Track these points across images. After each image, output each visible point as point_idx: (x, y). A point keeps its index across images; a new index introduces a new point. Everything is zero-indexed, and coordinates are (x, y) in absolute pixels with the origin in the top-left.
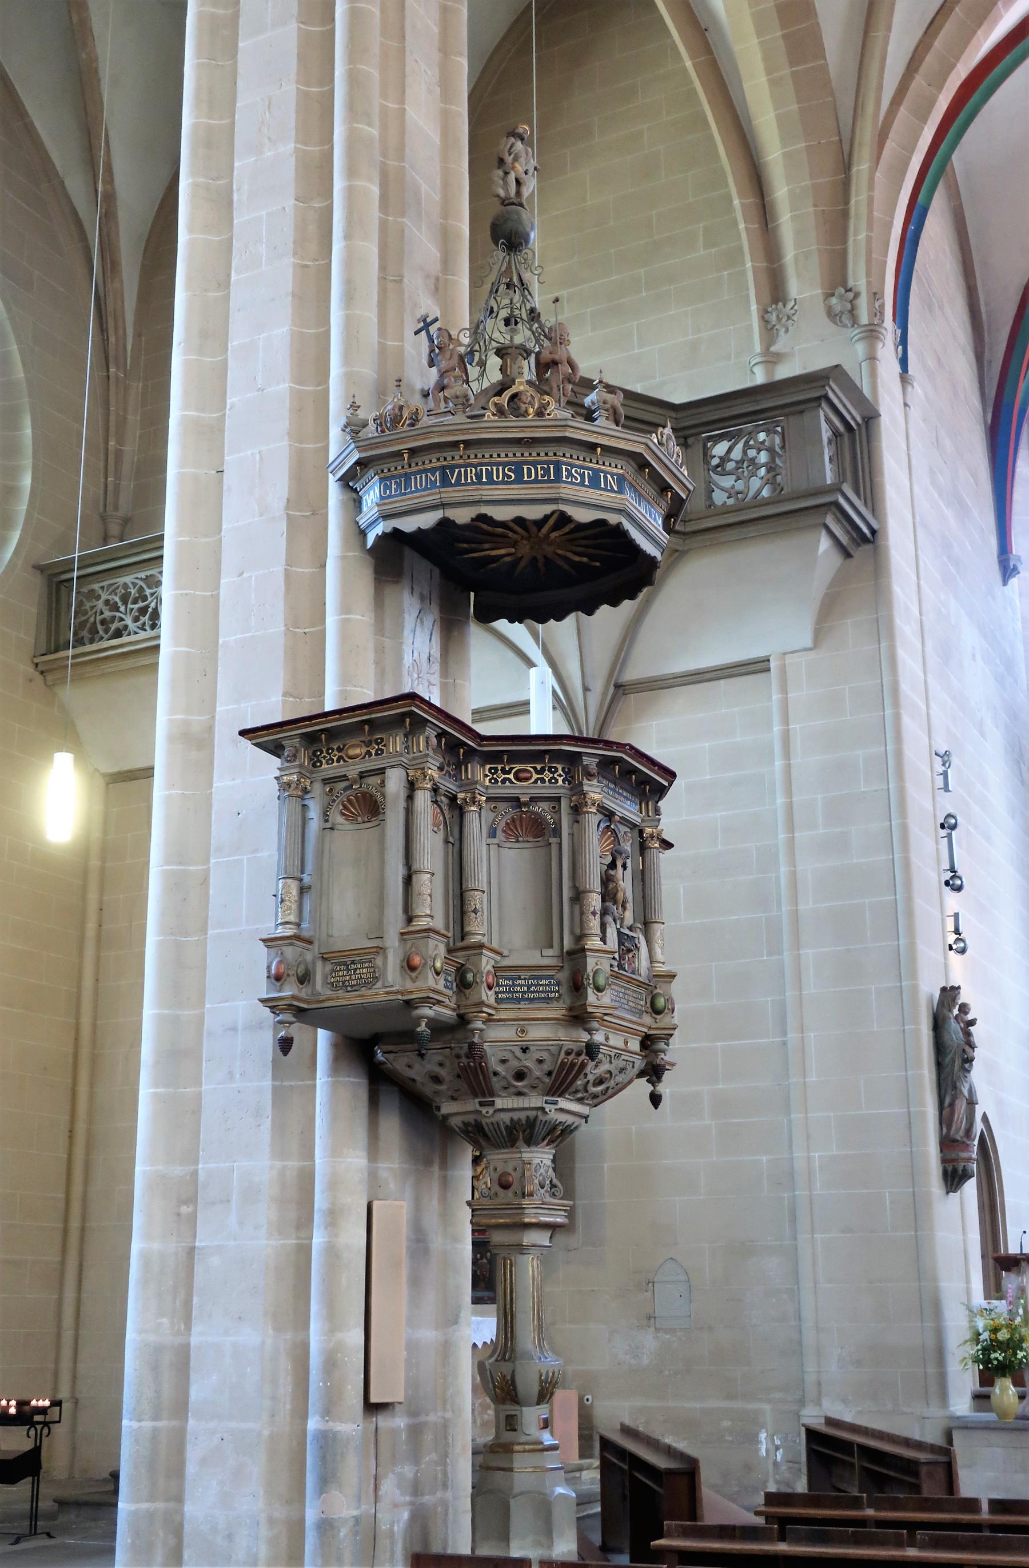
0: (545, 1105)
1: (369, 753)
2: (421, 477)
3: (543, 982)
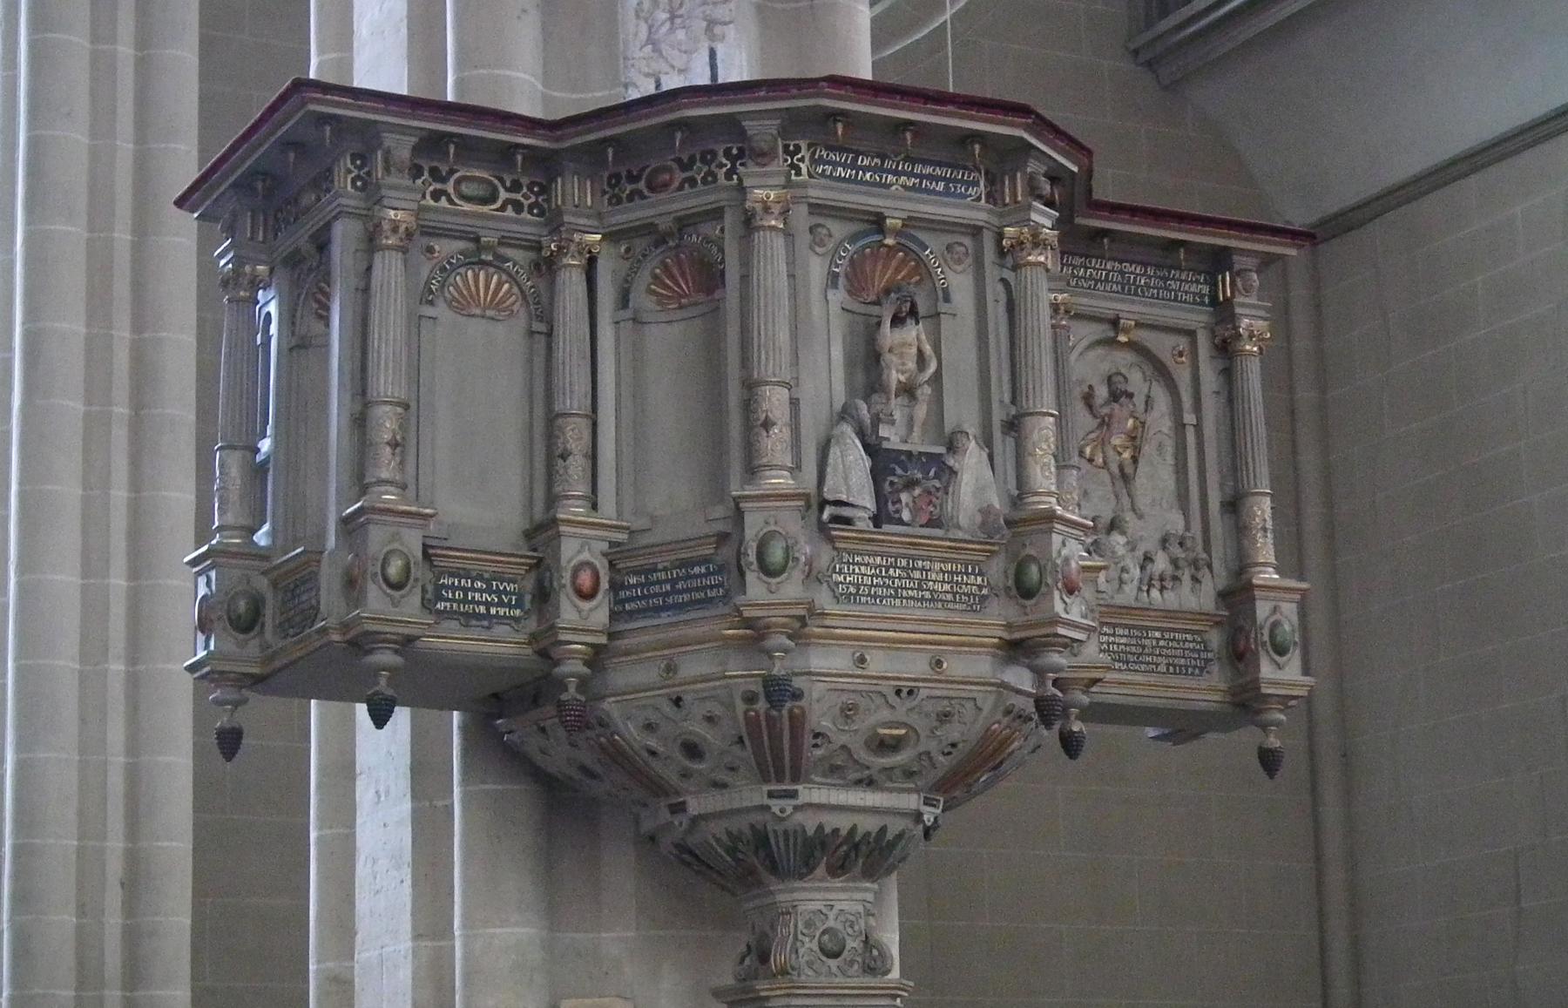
3: (697, 570)
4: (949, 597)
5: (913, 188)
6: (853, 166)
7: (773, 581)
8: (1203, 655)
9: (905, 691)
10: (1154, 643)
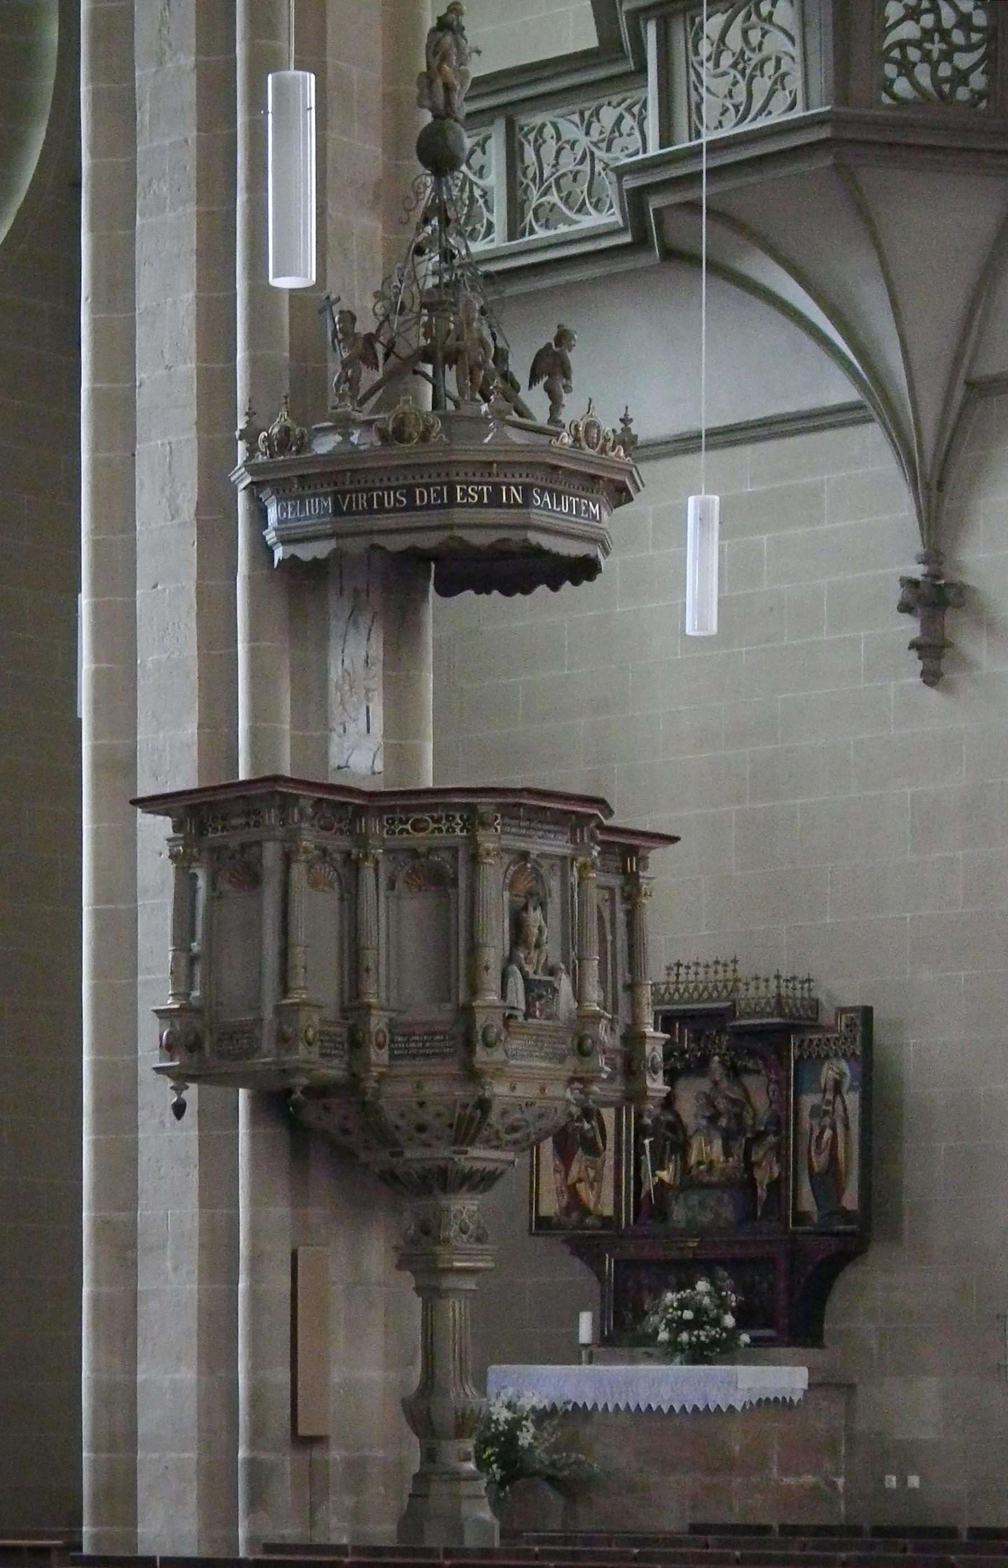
0: (453, 1156)
1: (248, 824)
2: (315, 501)
7: (489, 1050)
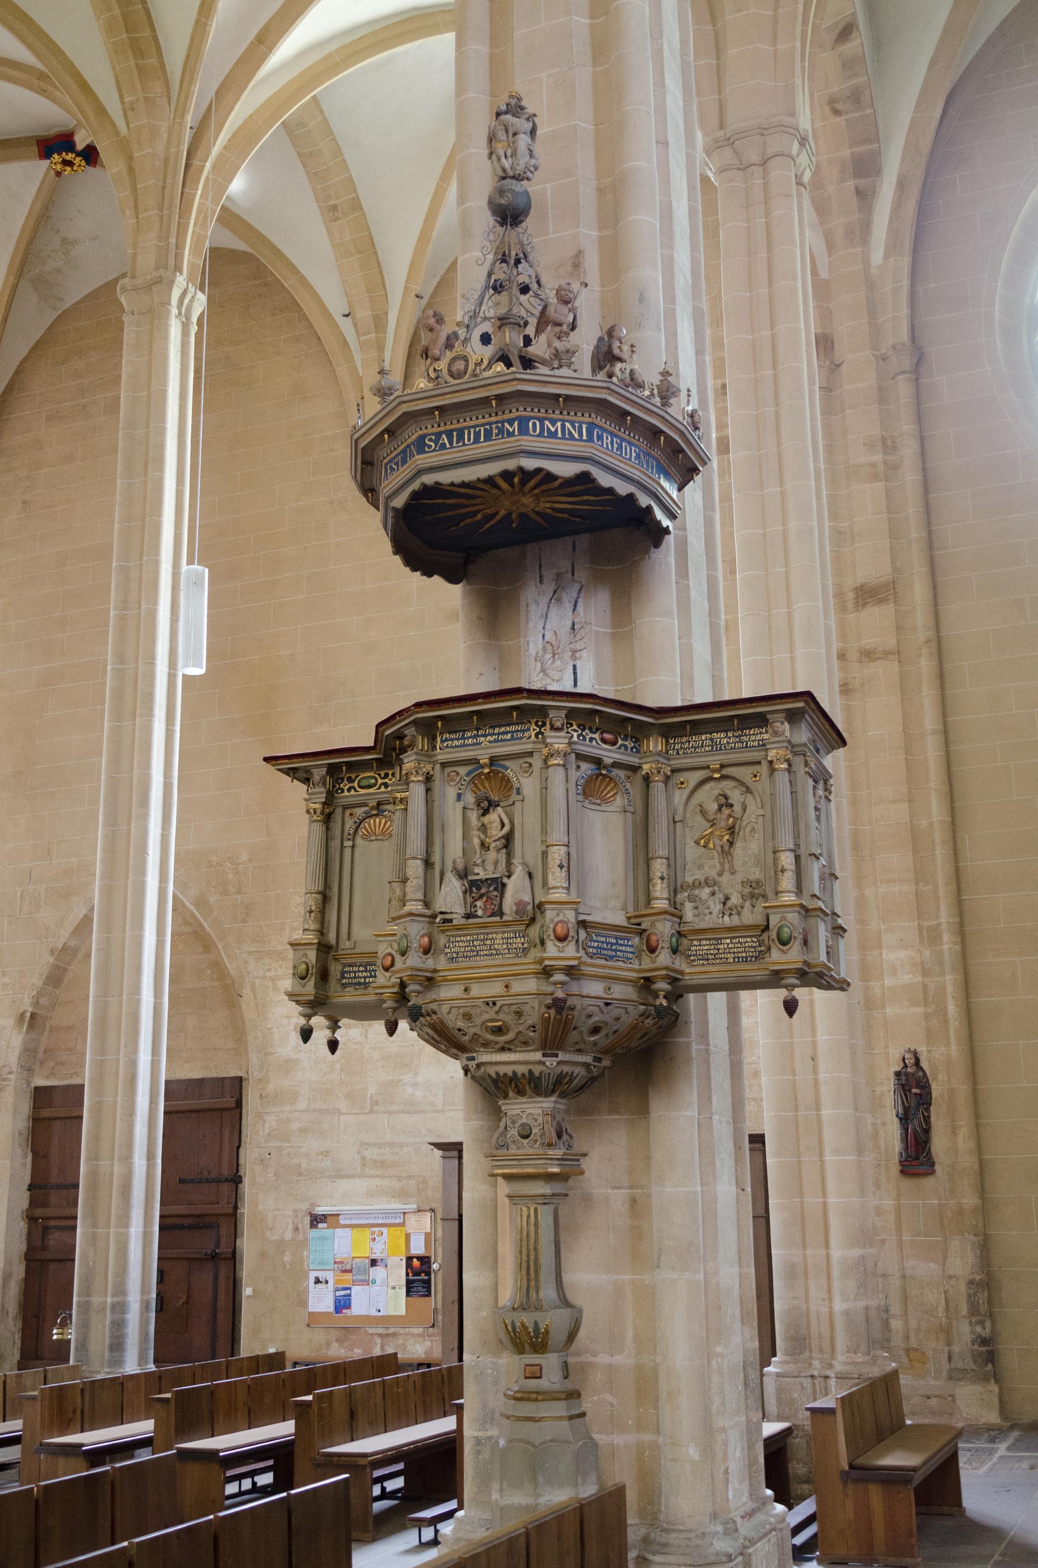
4: (506, 951)
5: (495, 741)
6: (463, 738)
8: (759, 949)
9: (490, 1003)
10: (726, 946)
